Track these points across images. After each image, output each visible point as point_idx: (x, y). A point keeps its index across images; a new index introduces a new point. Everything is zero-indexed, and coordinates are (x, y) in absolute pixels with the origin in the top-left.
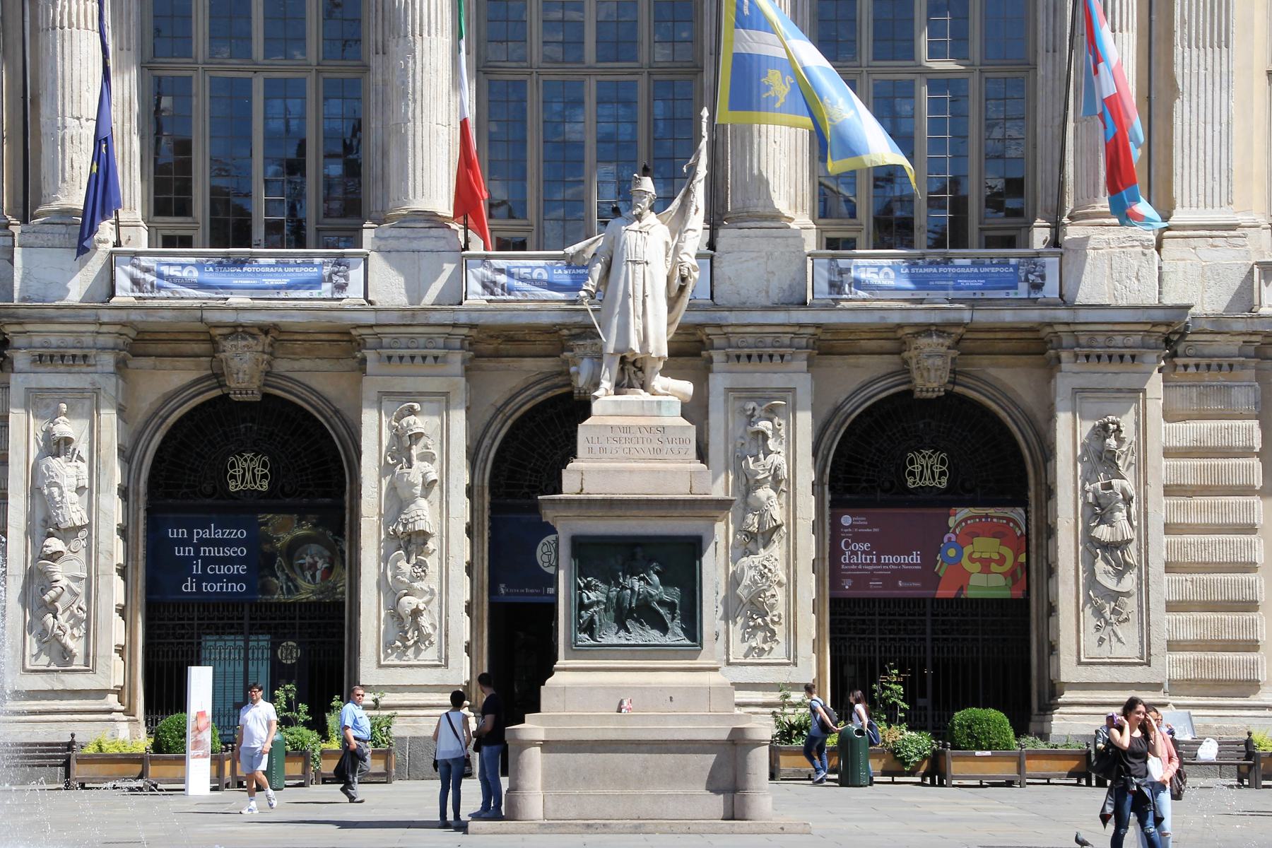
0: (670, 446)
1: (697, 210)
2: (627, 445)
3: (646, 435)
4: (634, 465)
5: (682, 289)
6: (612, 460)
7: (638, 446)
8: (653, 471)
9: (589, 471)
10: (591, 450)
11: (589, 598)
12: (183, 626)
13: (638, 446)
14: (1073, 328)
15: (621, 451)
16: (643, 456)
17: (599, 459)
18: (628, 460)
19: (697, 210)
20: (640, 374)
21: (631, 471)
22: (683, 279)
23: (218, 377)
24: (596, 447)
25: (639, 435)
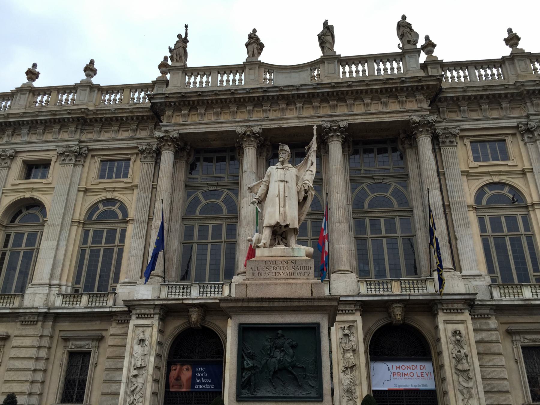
0: (299, 271)
1: (312, 164)
2: (274, 271)
3: (285, 265)
4: (278, 281)
5: (305, 198)
6: (264, 279)
7: (281, 272)
8: (288, 284)
9: (250, 284)
10: (253, 274)
11: (248, 364)
12: (189, 400)
13: (281, 272)
14: (441, 301)
15: (270, 275)
16: (284, 277)
17: (257, 279)
18: (276, 279)
19: (312, 164)
20: (284, 240)
21: (276, 284)
22: (306, 192)
23: (189, 322)
24: (256, 272)
25: (281, 265)
